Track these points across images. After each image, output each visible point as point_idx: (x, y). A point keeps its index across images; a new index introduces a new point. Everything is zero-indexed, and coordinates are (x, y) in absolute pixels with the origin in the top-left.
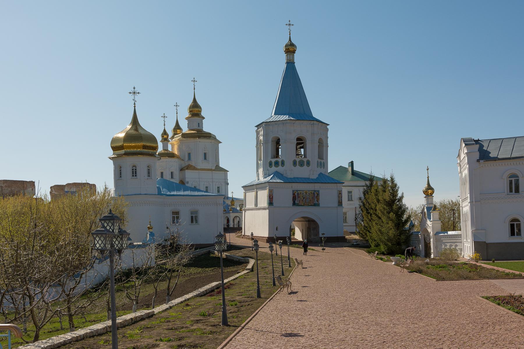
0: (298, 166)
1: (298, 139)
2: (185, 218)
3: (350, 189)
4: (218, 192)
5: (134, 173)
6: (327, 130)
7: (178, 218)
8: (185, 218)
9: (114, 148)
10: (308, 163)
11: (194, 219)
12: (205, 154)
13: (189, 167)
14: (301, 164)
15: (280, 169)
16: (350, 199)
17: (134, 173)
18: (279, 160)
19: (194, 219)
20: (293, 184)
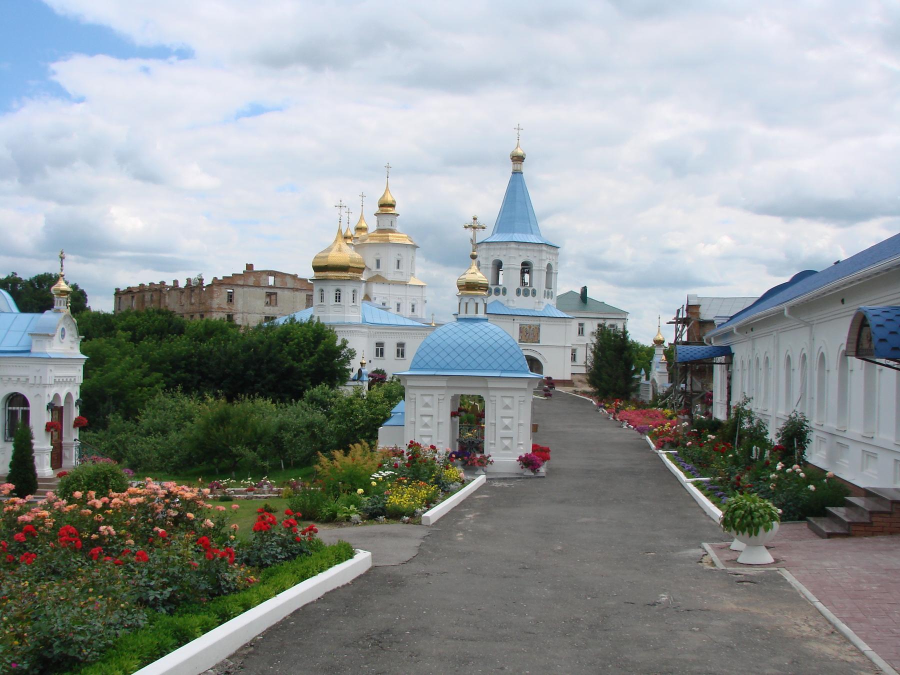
0: (521, 296)
1: (524, 264)
2: (390, 350)
3: (581, 321)
4: (413, 310)
5: (338, 298)
6: (558, 254)
7: (382, 351)
8: (390, 350)
9: (317, 269)
10: (534, 293)
11: (401, 352)
12: (398, 261)
13: (378, 279)
14: (526, 294)
15: (500, 297)
16: (581, 332)
17: (338, 298)
18: (501, 288)
19: (401, 352)
20: (516, 318)
